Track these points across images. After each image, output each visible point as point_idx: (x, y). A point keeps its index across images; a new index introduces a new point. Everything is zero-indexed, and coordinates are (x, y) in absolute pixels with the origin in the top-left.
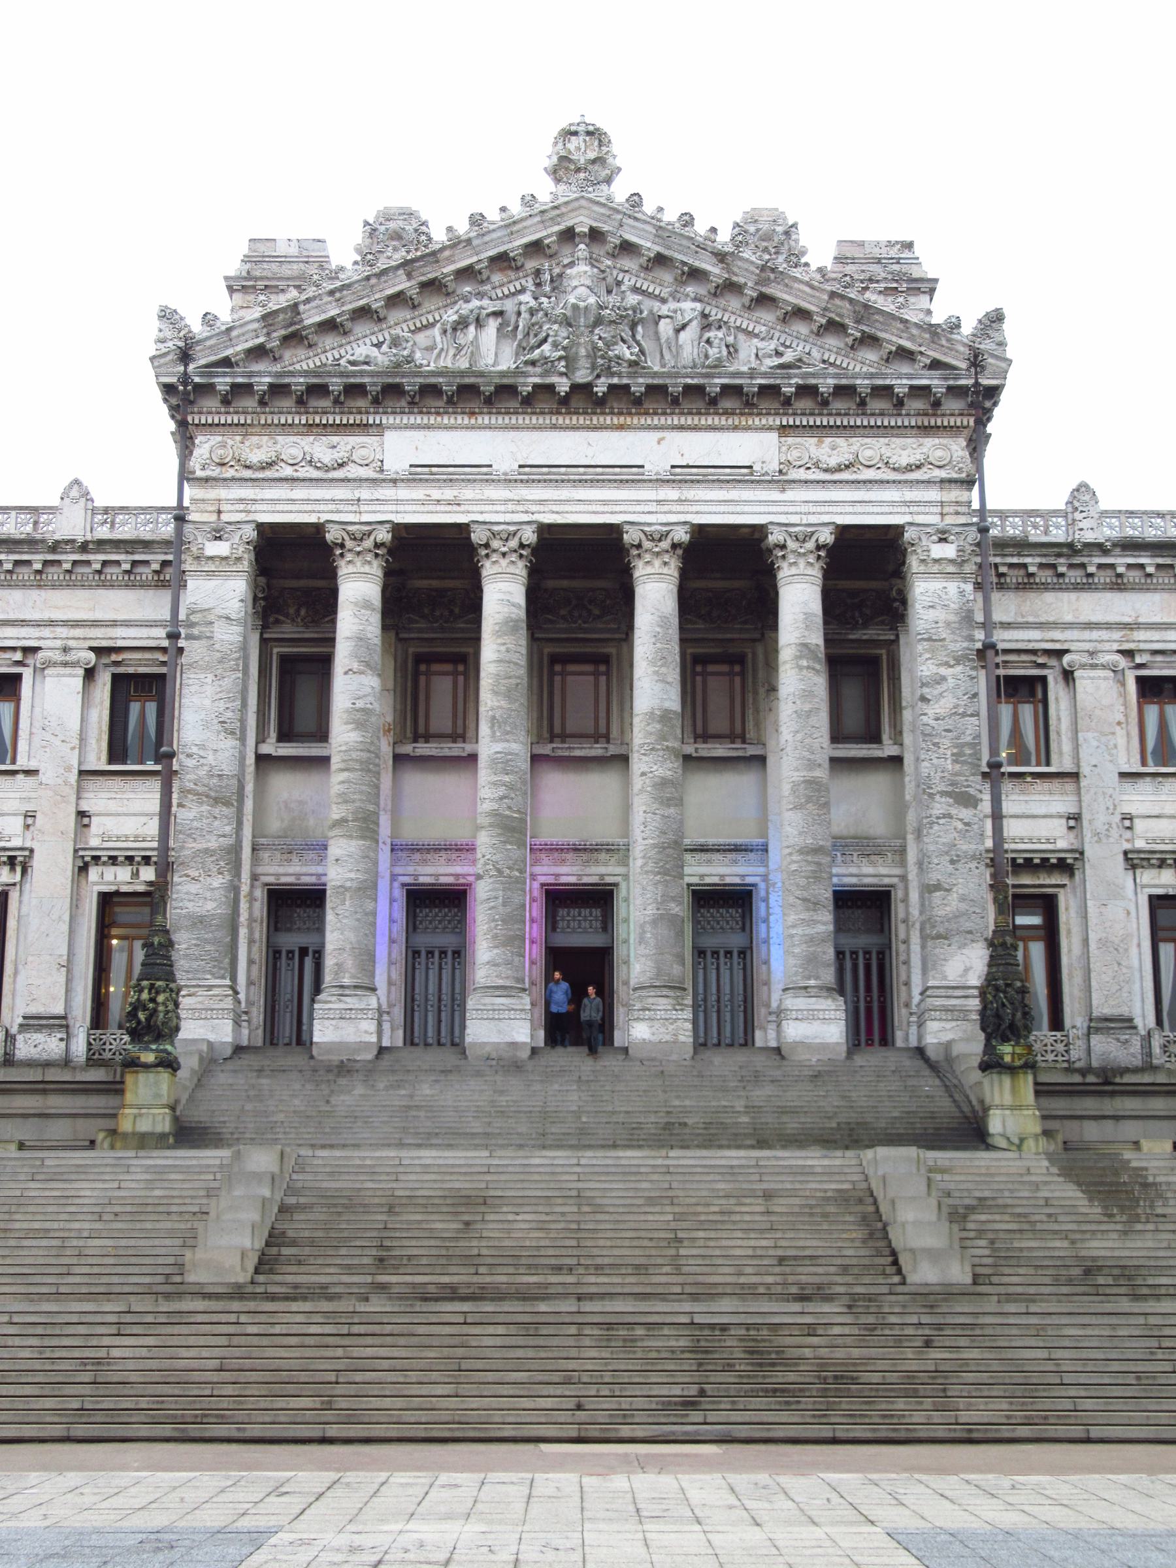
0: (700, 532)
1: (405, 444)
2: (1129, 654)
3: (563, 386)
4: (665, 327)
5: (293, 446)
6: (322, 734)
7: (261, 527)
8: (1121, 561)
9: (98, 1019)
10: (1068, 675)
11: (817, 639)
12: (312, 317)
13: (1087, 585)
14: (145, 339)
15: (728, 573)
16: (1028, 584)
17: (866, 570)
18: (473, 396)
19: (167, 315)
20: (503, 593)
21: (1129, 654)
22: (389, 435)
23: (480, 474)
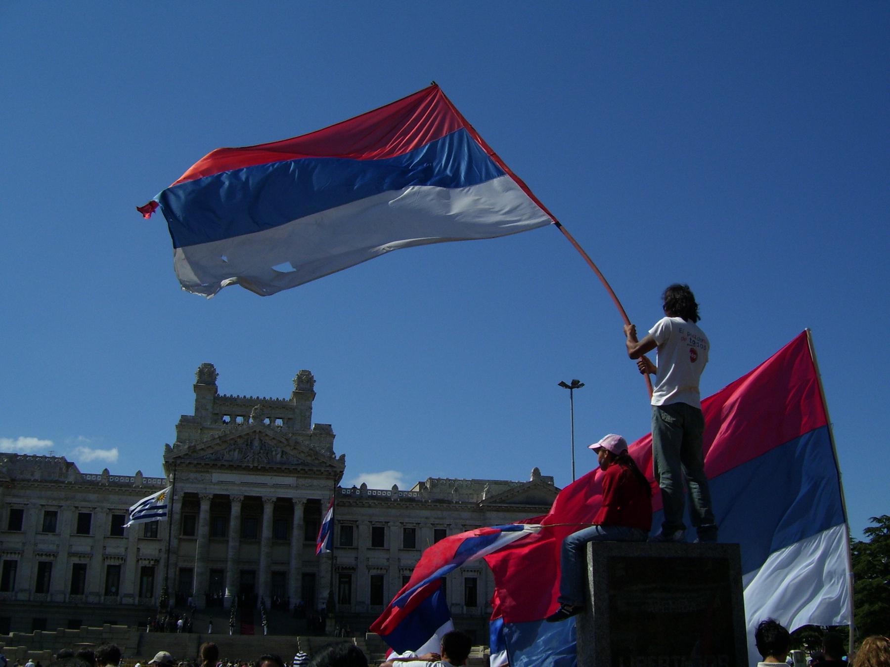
0: (279, 499)
1: (216, 476)
2: (371, 522)
3: (251, 466)
4: (274, 453)
5: (192, 476)
6: (192, 534)
7: (185, 493)
8: (371, 502)
9: (140, 596)
10: (358, 527)
11: (302, 523)
12: (199, 447)
13: (363, 506)
14: (162, 451)
15: (284, 507)
16: (350, 505)
17: (314, 508)
18: (233, 467)
19: (167, 446)
20: (236, 509)
21: (371, 522)
22: (214, 475)
23: (233, 483)
